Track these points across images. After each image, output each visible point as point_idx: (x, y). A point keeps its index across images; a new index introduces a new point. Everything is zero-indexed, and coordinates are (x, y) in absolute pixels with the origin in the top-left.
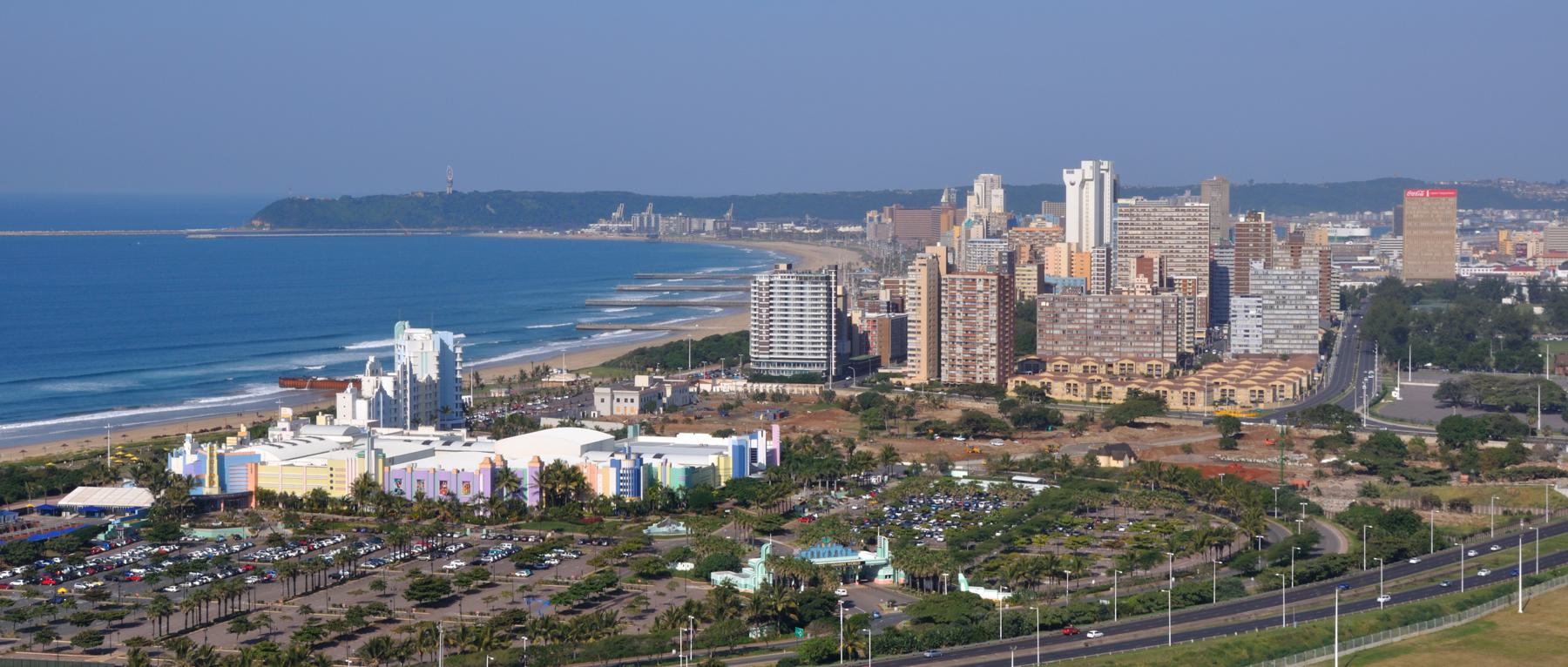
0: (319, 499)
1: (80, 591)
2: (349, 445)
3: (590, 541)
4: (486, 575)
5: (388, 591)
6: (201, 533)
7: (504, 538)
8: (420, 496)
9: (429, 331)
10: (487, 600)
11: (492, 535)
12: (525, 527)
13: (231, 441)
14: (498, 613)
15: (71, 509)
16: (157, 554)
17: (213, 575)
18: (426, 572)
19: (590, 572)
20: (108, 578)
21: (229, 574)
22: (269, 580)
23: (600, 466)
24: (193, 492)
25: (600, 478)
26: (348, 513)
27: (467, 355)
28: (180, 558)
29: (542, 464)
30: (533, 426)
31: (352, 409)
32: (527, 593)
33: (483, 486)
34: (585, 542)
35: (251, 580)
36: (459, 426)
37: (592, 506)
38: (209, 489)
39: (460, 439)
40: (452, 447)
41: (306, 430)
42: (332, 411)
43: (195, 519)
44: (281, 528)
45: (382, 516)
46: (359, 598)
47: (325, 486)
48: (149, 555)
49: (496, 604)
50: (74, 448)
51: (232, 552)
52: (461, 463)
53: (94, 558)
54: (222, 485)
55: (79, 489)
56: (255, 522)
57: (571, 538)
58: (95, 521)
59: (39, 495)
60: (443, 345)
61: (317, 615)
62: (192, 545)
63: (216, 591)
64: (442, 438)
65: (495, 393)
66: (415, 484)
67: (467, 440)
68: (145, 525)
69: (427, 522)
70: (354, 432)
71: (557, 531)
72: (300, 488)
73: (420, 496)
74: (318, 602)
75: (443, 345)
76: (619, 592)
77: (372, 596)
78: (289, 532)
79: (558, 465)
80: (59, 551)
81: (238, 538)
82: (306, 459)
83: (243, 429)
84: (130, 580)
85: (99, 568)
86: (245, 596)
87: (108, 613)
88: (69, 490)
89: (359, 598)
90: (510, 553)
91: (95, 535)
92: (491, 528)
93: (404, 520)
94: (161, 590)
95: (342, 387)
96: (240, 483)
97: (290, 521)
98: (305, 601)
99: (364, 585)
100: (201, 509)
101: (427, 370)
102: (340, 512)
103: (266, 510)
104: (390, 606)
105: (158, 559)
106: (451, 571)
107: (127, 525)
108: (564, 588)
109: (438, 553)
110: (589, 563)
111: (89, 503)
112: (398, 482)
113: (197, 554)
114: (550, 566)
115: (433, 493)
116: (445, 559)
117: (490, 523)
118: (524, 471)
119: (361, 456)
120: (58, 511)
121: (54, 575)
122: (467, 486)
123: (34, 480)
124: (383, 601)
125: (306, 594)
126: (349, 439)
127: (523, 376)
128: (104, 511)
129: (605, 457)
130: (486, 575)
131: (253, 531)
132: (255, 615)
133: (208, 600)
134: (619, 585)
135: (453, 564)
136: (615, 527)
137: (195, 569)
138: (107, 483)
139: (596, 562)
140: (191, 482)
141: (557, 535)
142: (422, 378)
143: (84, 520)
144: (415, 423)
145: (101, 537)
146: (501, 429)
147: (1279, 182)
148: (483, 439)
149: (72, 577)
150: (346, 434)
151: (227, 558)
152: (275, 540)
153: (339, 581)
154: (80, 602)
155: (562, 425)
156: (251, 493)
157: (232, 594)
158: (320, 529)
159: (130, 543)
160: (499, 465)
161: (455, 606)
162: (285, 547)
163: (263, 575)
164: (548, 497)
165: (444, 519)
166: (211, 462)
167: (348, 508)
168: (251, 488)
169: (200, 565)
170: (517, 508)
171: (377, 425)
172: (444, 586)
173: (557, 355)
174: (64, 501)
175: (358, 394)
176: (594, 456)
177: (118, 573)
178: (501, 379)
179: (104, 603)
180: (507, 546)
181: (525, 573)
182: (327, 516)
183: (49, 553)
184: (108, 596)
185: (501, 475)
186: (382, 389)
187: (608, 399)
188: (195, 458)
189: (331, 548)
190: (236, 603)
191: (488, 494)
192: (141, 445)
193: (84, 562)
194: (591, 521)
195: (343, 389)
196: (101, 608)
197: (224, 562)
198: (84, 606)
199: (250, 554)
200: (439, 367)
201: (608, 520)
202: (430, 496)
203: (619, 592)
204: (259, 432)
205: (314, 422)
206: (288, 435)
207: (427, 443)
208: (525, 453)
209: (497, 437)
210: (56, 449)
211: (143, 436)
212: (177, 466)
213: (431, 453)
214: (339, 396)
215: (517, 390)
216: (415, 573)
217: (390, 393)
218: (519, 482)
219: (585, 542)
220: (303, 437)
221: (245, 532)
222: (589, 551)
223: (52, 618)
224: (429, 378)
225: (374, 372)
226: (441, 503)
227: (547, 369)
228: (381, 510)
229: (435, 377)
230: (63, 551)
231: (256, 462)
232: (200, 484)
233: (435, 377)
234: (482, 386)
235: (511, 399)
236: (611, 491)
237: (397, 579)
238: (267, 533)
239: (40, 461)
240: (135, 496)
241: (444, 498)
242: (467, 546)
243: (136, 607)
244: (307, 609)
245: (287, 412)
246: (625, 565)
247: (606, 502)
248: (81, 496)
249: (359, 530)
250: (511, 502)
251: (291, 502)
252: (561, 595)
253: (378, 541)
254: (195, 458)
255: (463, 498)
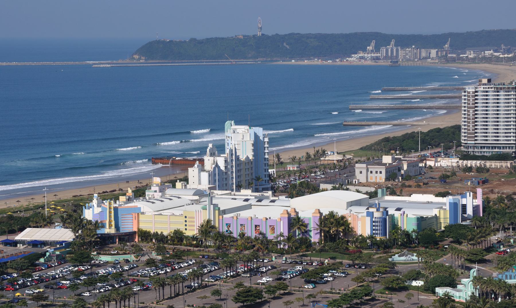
0: (178, 237)
1: (29, 295)
2: (197, 202)
4: (285, 287)
5: (222, 297)
6: (104, 258)
7: (297, 263)
8: (242, 235)
9: (247, 127)
11: (289, 261)
12: (311, 256)
13: (122, 199)
15: (23, 242)
16: (78, 271)
18: (247, 284)
19: (354, 286)
20: (46, 287)
22: (147, 289)
23: (360, 216)
24: (99, 232)
25: (360, 224)
26: (196, 246)
28: (91, 274)
29: (321, 214)
30: (314, 189)
31: (198, 178)
33: (283, 228)
34: (350, 266)
35: (136, 289)
36: (267, 189)
37: (354, 242)
39: (267, 198)
41: (169, 192)
42: (186, 180)
43: (100, 249)
44: (154, 255)
45: (219, 248)
46: (205, 301)
47: (182, 228)
48: (72, 272)
50: (24, 203)
52: (269, 213)
54: (117, 227)
55: (28, 230)
56: (138, 251)
57: (341, 263)
58: (38, 250)
60: (256, 136)
62: (99, 266)
63: (114, 296)
64: (256, 197)
65: (290, 168)
66: (239, 227)
68: (69, 253)
69: (247, 252)
70: (200, 193)
72: (166, 229)
73: (242, 235)
75: (256, 136)
78: (160, 258)
79: (332, 215)
81: (127, 261)
82: (170, 210)
83: (130, 191)
84: (60, 288)
85: (41, 280)
86: (132, 299)
88: (22, 230)
89: (205, 301)
90: (301, 273)
91: (38, 259)
92: (289, 256)
93: (233, 251)
94: (80, 295)
95: (191, 164)
96: (129, 226)
97: (160, 250)
99: (207, 292)
100: (104, 242)
101: (246, 153)
102: (191, 245)
103: (145, 244)
105: (77, 274)
107: (58, 253)
108: (337, 297)
109: (255, 272)
110: (353, 280)
112: (228, 225)
113: (102, 272)
114: (328, 281)
115: (251, 233)
116: (259, 276)
117: (288, 253)
118: (309, 219)
119: (204, 209)
120: (15, 243)
121: (13, 285)
122: (273, 229)
124: (220, 303)
125: (171, 298)
126: (197, 198)
127: (308, 156)
128: (44, 243)
129: (363, 210)
130: (285, 287)
131: (137, 257)
133: (109, 301)
135: (264, 280)
136: (370, 256)
137: (101, 281)
138: (45, 226)
139: (358, 279)
140: (98, 225)
142: (243, 158)
143: (31, 250)
144: (239, 187)
145: (42, 260)
148: (282, 198)
149: (24, 286)
151: (121, 274)
152: (151, 263)
154: (29, 302)
155: (334, 188)
156: (135, 233)
158: (179, 256)
159: (60, 264)
160: (293, 215)
163: (143, 285)
164: (325, 236)
165: (258, 250)
166: (110, 212)
167: (197, 242)
168: (135, 229)
169: (104, 279)
170: (305, 243)
171: (214, 188)
174: (19, 237)
175: (202, 169)
177: (53, 284)
178: (294, 159)
180: (299, 268)
182: (183, 248)
183: (10, 271)
185: (295, 222)
186: (217, 165)
187: (364, 171)
188: (100, 209)
191: (286, 234)
192: (66, 201)
194: (354, 252)
195: (192, 166)
197: (118, 277)
200: (254, 150)
202: (249, 235)
204: (140, 193)
205: (174, 186)
206: (158, 195)
207: (247, 200)
208: (309, 207)
209: (291, 196)
210: (13, 204)
211: (67, 195)
212: (88, 214)
213: (249, 207)
214: (190, 170)
215: (304, 165)
216: (240, 285)
217: (223, 168)
219: (350, 266)
221: (132, 258)
222: (352, 272)
224: (248, 158)
225: (212, 154)
227: (324, 152)
228: (217, 243)
229: (251, 157)
230: (18, 269)
231: (139, 213)
232: (103, 226)
233: (251, 157)
234: (282, 163)
235: (301, 171)
236: (367, 232)
238: (145, 258)
240: (63, 234)
242: (273, 267)
245: (157, 180)
246: (377, 282)
247: (363, 239)
248: (29, 234)
249: (203, 257)
250: (301, 239)
251: (161, 238)
252: (335, 301)
253: (216, 264)
254: (100, 209)
255: (270, 236)
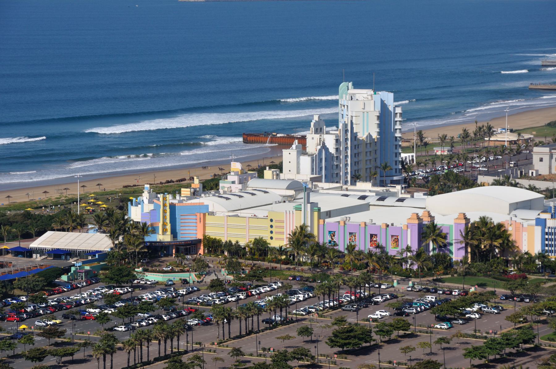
0: (260, 249)
1: (40, 328)
2: (291, 199)
3: (512, 298)
4: (406, 326)
5: (314, 338)
6: (152, 277)
7: (428, 291)
8: (351, 248)
9: (371, 92)
10: (405, 350)
11: (418, 287)
12: (450, 280)
13: (185, 192)
14: (413, 363)
15: (41, 251)
16: (112, 295)
17: (159, 317)
18: (352, 319)
19: (509, 328)
20: (66, 317)
21: (175, 315)
22: (208, 323)
23: (525, 224)
24: (147, 239)
25: (525, 236)
26: (286, 262)
27: (407, 116)
28: (132, 299)
29: (467, 220)
30: (469, 183)
31: (297, 165)
32: (445, 345)
33: (411, 240)
34: (507, 297)
35: (193, 322)
36: (397, 182)
37: (517, 263)
38: (165, 238)
39: (394, 194)
40: (387, 202)
41: (254, 183)
42: (279, 167)
43: (148, 263)
44: (225, 275)
45: (316, 266)
46: (287, 343)
47: (266, 236)
48: (105, 296)
49: (413, 355)
50: (54, 195)
51: (178, 295)
52: (391, 217)
53: (56, 297)
54: (174, 233)
55: (49, 233)
56: (202, 268)
57: (493, 293)
58: (60, 263)
59: (14, 238)
60: (383, 105)
61: (247, 358)
62: (144, 288)
63: (155, 333)
64: (377, 193)
65: (439, 152)
66: (348, 237)
67: (401, 196)
68: (104, 268)
69: (357, 273)
70: (295, 186)
71: (481, 285)
72: (244, 240)
73: (351, 248)
74: (248, 346)
75: (383, 105)
76: (537, 348)
77: (298, 341)
78: (231, 278)
79: (484, 221)
80: (26, 290)
81: (185, 282)
82: (250, 211)
83: (196, 181)
84: (85, 319)
85: (59, 307)
86: (183, 337)
87: (60, 349)
88: (40, 234)
89: (287, 343)
90: (433, 304)
91: (59, 276)
92: (417, 280)
93: (336, 271)
94: (111, 329)
95: (287, 143)
96: (190, 232)
97: (232, 268)
98: (236, 343)
99: (292, 331)
100: (154, 254)
101: (368, 129)
102: (278, 261)
103: (213, 257)
104: (313, 352)
105: (110, 300)
106: (375, 320)
107: (87, 268)
108: (480, 343)
109: (366, 302)
110: (508, 318)
111: (56, 246)
112: (332, 234)
113: (147, 296)
114: (470, 319)
115: (363, 245)
116: (372, 307)
117: (416, 276)
118: (450, 227)
119: (298, 209)
120: (29, 253)
121: (19, 313)
122: (396, 241)
123: (11, 224)
124: (307, 346)
125: (240, 336)
126: (291, 192)
127: (466, 135)
128: (69, 254)
129: (533, 215)
130: (406, 326)
131: (199, 276)
132: (191, 355)
133: (149, 341)
134: (536, 341)
135: (378, 314)
136: (537, 285)
137: (143, 310)
138: (74, 229)
139: (514, 318)
140: (144, 229)
141: (480, 290)
142: (362, 136)
143: (52, 262)
144: (356, 178)
145: (64, 278)
146: (437, 185)
147: (164, 128)
148: (419, 195)
149: (34, 315)
150: (288, 188)
151: (172, 301)
152: (217, 285)
153: (272, 324)
154: (37, 338)
155: (497, 183)
156: (199, 241)
157: (170, 335)
158: (258, 276)
159: (89, 284)
160: (426, 221)
161: (374, 354)
162: (226, 292)
163: (203, 317)
164: (473, 254)
165: (374, 271)
166: (164, 212)
167: (287, 257)
168: (200, 237)
169: (147, 307)
170: (443, 263)
171: (319, 180)
172: (366, 335)
173: (499, 115)
174: (35, 244)
175: (303, 150)
176: (522, 214)
177: (75, 313)
178: (443, 138)
179: (59, 340)
180: (430, 298)
181: (445, 326)
182: (266, 264)
183: (17, 292)
184: (62, 334)
185: (428, 231)
186: (324, 147)
187: (546, 158)
188: (152, 207)
189: (265, 294)
190: (175, 343)
191: (415, 247)
192: (112, 193)
193: (45, 301)
194: (515, 277)
195: (288, 146)
196: (57, 344)
197: (168, 304)
198: (40, 342)
199: (194, 297)
200: (380, 126)
201: (532, 277)
202: (362, 248)
203: (537, 348)
204: (211, 185)
205: (261, 175)
206: (236, 188)
207: (363, 198)
208: (451, 209)
209: (432, 193)
210: (38, 196)
211: (115, 186)
212: (135, 214)
213: (366, 208)
214: (285, 152)
215: (460, 148)
216: (341, 321)
217: (332, 150)
218: (445, 237)
219: (507, 297)
220: (249, 190)
221: (192, 277)
222: (510, 307)
223: (11, 353)
224: (370, 136)
225: (319, 130)
226: (370, 255)
227: (490, 128)
228: (313, 258)
229: (375, 136)
230: (30, 290)
231: (205, 212)
232: (154, 231)
233: (375, 136)
234: (426, 144)
235: (451, 157)
236: (536, 249)
237: (323, 326)
238: (208, 279)
239: (22, 206)
240: (97, 241)
241: (374, 250)
242: (393, 297)
243: (85, 345)
244: (237, 352)
245: (236, 166)
246: (544, 322)
247: (530, 259)
248: (50, 240)
249: (294, 278)
250: (436, 256)
251: (236, 251)
252: (476, 349)
253: (310, 289)
254: (152, 207)
255: (392, 251)
